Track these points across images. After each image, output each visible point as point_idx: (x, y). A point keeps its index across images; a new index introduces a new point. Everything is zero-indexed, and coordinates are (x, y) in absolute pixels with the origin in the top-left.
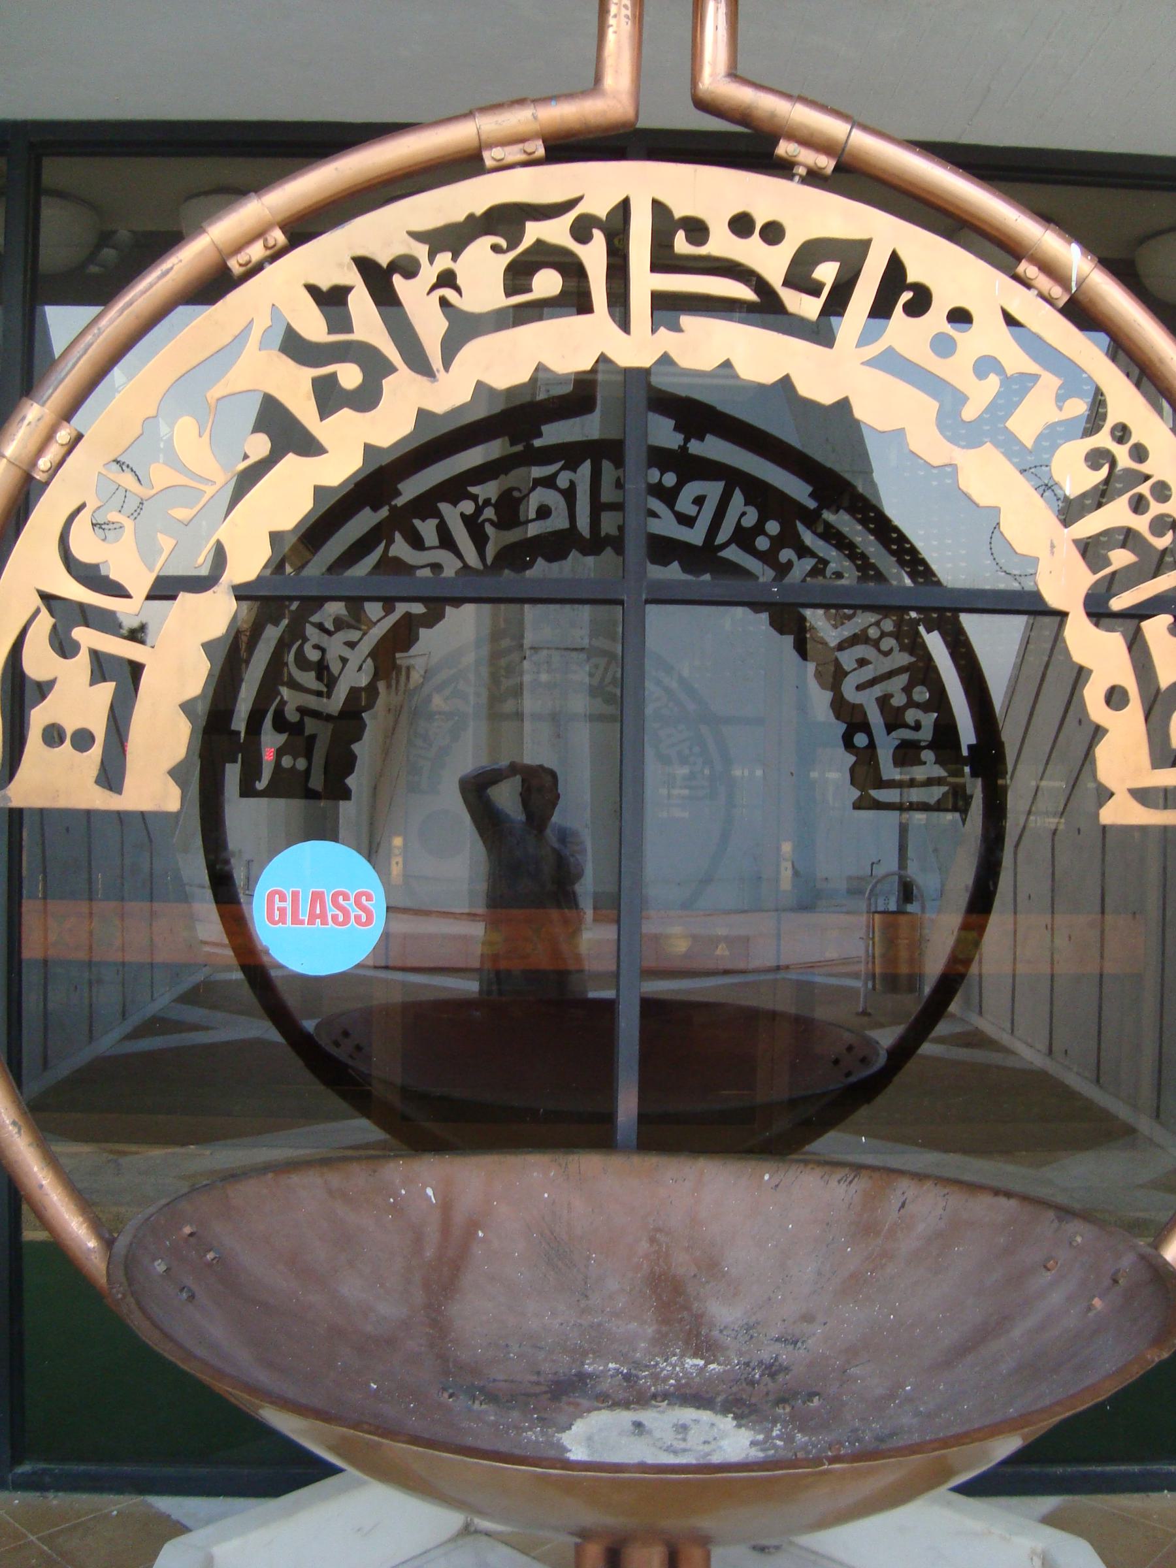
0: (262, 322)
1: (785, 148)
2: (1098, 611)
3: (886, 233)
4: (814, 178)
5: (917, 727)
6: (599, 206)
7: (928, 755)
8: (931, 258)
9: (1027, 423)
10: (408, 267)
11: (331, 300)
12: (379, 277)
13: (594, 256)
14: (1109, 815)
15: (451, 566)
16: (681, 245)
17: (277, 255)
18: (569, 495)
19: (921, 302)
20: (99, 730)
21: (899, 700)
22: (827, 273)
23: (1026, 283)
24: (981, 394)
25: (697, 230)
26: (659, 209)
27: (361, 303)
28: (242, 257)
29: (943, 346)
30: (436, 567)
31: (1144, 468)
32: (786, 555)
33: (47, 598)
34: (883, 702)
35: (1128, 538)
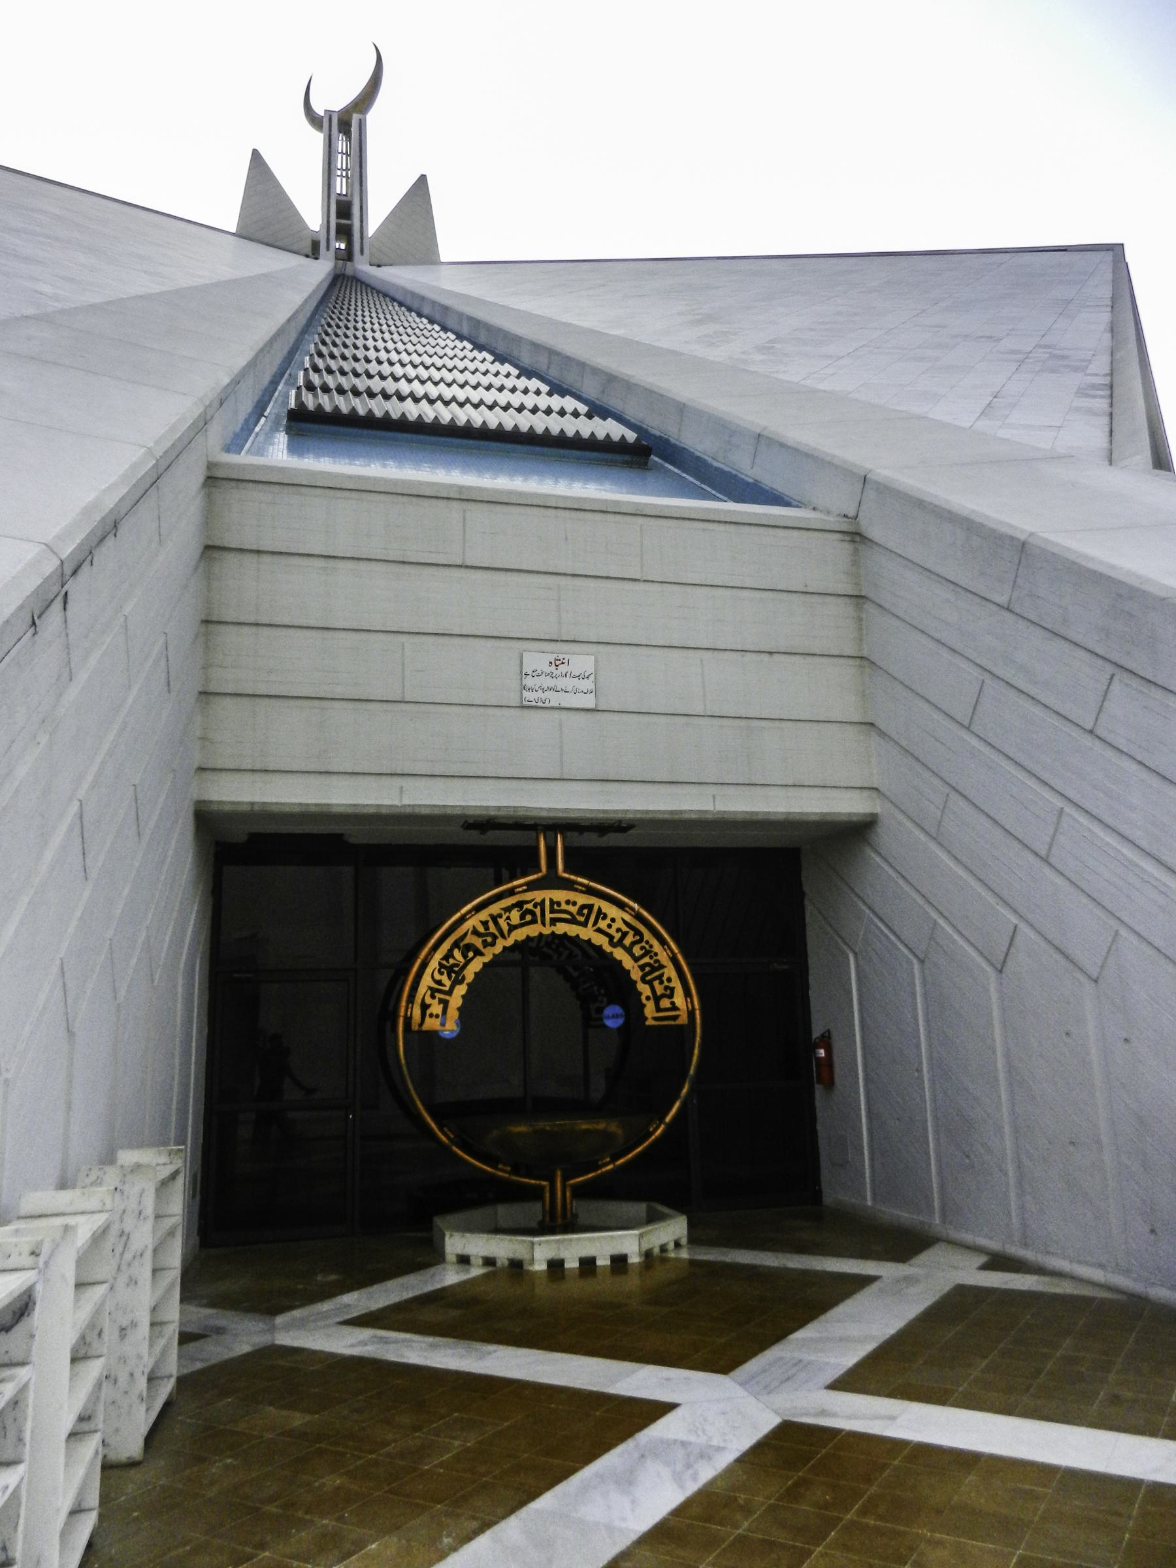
2: (643, 980)
4: (581, 892)
6: (538, 900)
9: (628, 941)
10: (500, 916)
11: (485, 924)
12: (494, 918)
13: (538, 911)
22: (585, 911)
24: (617, 936)
25: (559, 904)
26: (551, 900)
27: (491, 924)
29: (609, 926)
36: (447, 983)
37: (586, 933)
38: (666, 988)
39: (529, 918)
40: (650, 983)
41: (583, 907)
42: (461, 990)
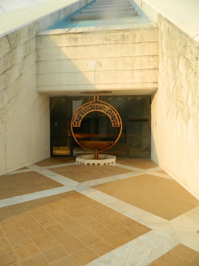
4: (102, 104)
12: (86, 108)
13: (94, 107)
14: (112, 126)
22: (102, 107)
24: (107, 111)
26: (96, 105)
27: (86, 109)
29: (106, 110)
35: (113, 116)
36: (79, 119)
37: (102, 111)
38: (116, 120)
39: (92, 108)
40: (113, 119)
41: (102, 106)
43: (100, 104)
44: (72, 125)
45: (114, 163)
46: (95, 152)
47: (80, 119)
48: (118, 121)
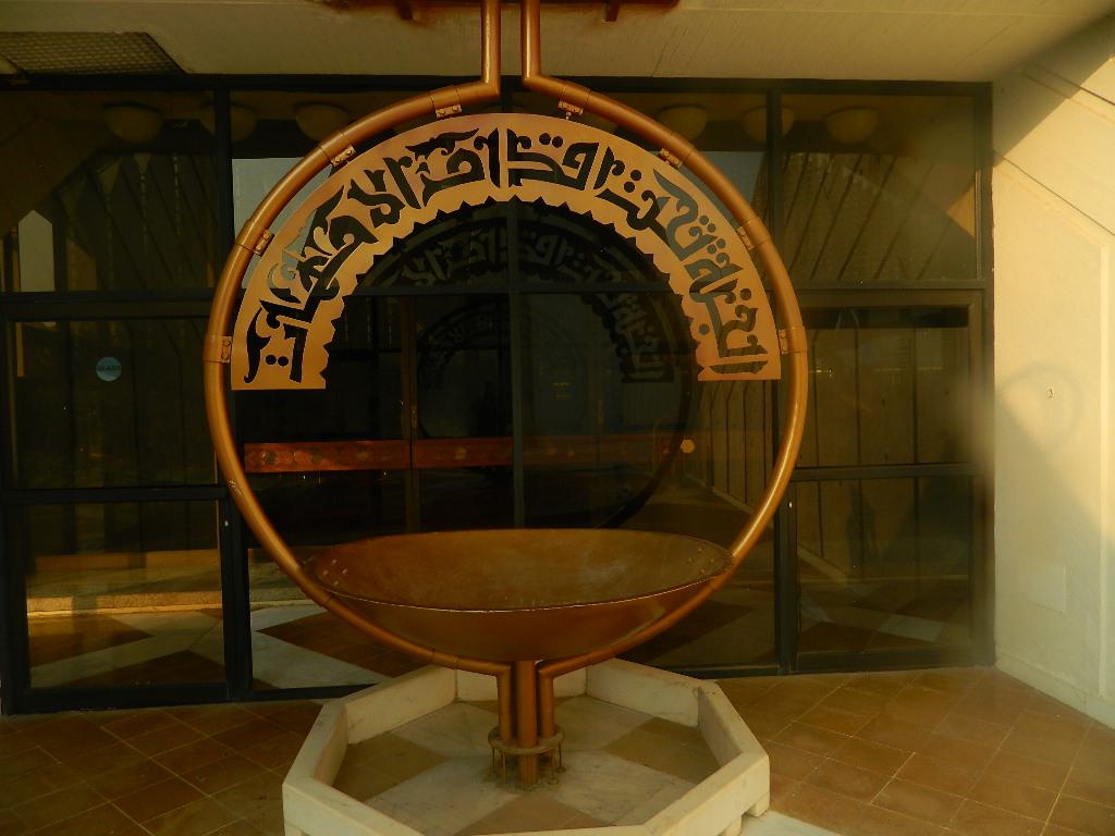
0: (348, 187)
1: (562, 105)
3: (606, 140)
4: (575, 117)
5: (650, 344)
6: (485, 133)
7: (656, 357)
8: (625, 150)
9: (663, 219)
10: (407, 162)
12: (394, 166)
13: (484, 155)
14: (702, 377)
15: (431, 279)
16: (520, 148)
17: (351, 157)
18: (486, 244)
19: (620, 169)
20: (290, 357)
21: (642, 332)
22: (580, 158)
23: (663, 158)
24: (644, 208)
25: (526, 142)
26: (510, 133)
27: (388, 179)
28: (337, 159)
29: (629, 187)
30: (424, 281)
31: (713, 234)
32: (588, 268)
33: (264, 303)
34: (635, 334)
36: (303, 296)
37: (584, 201)
38: (739, 310)
39: (465, 167)
41: (576, 148)
42: (331, 310)
43: (553, 126)
44: (226, 369)
45: (758, 811)
46: (505, 668)
47: (320, 295)
48: (765, 315)
